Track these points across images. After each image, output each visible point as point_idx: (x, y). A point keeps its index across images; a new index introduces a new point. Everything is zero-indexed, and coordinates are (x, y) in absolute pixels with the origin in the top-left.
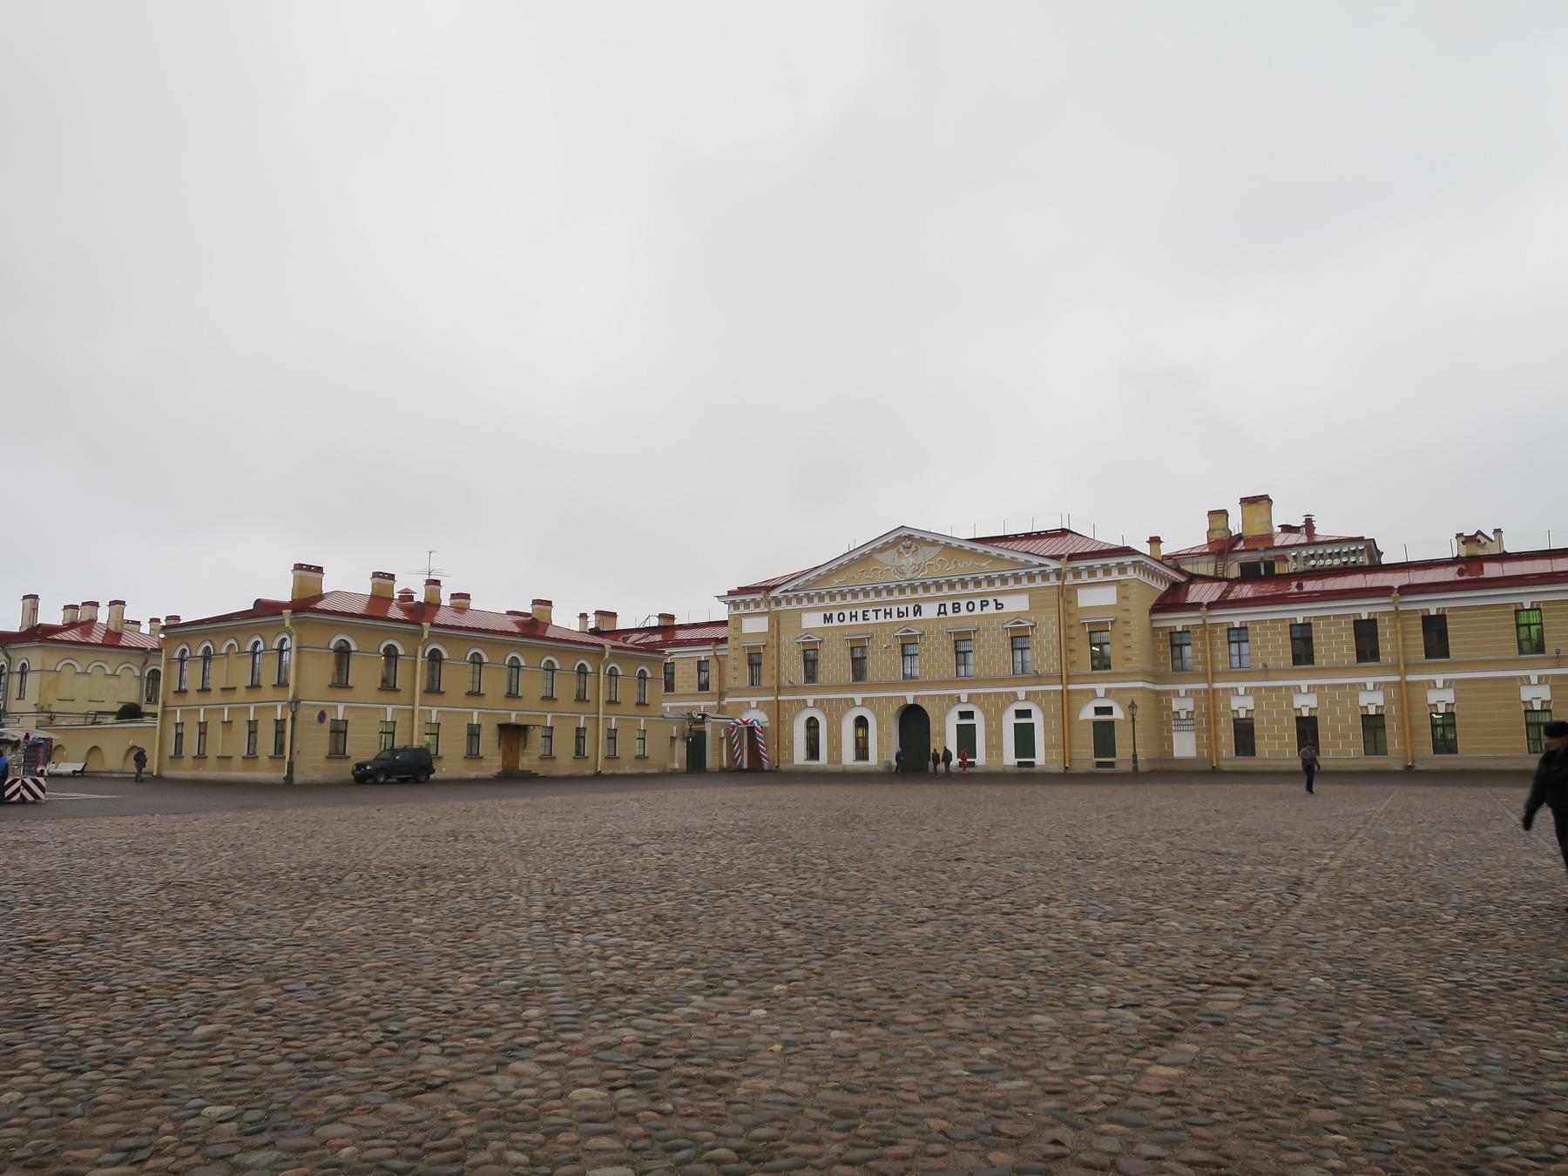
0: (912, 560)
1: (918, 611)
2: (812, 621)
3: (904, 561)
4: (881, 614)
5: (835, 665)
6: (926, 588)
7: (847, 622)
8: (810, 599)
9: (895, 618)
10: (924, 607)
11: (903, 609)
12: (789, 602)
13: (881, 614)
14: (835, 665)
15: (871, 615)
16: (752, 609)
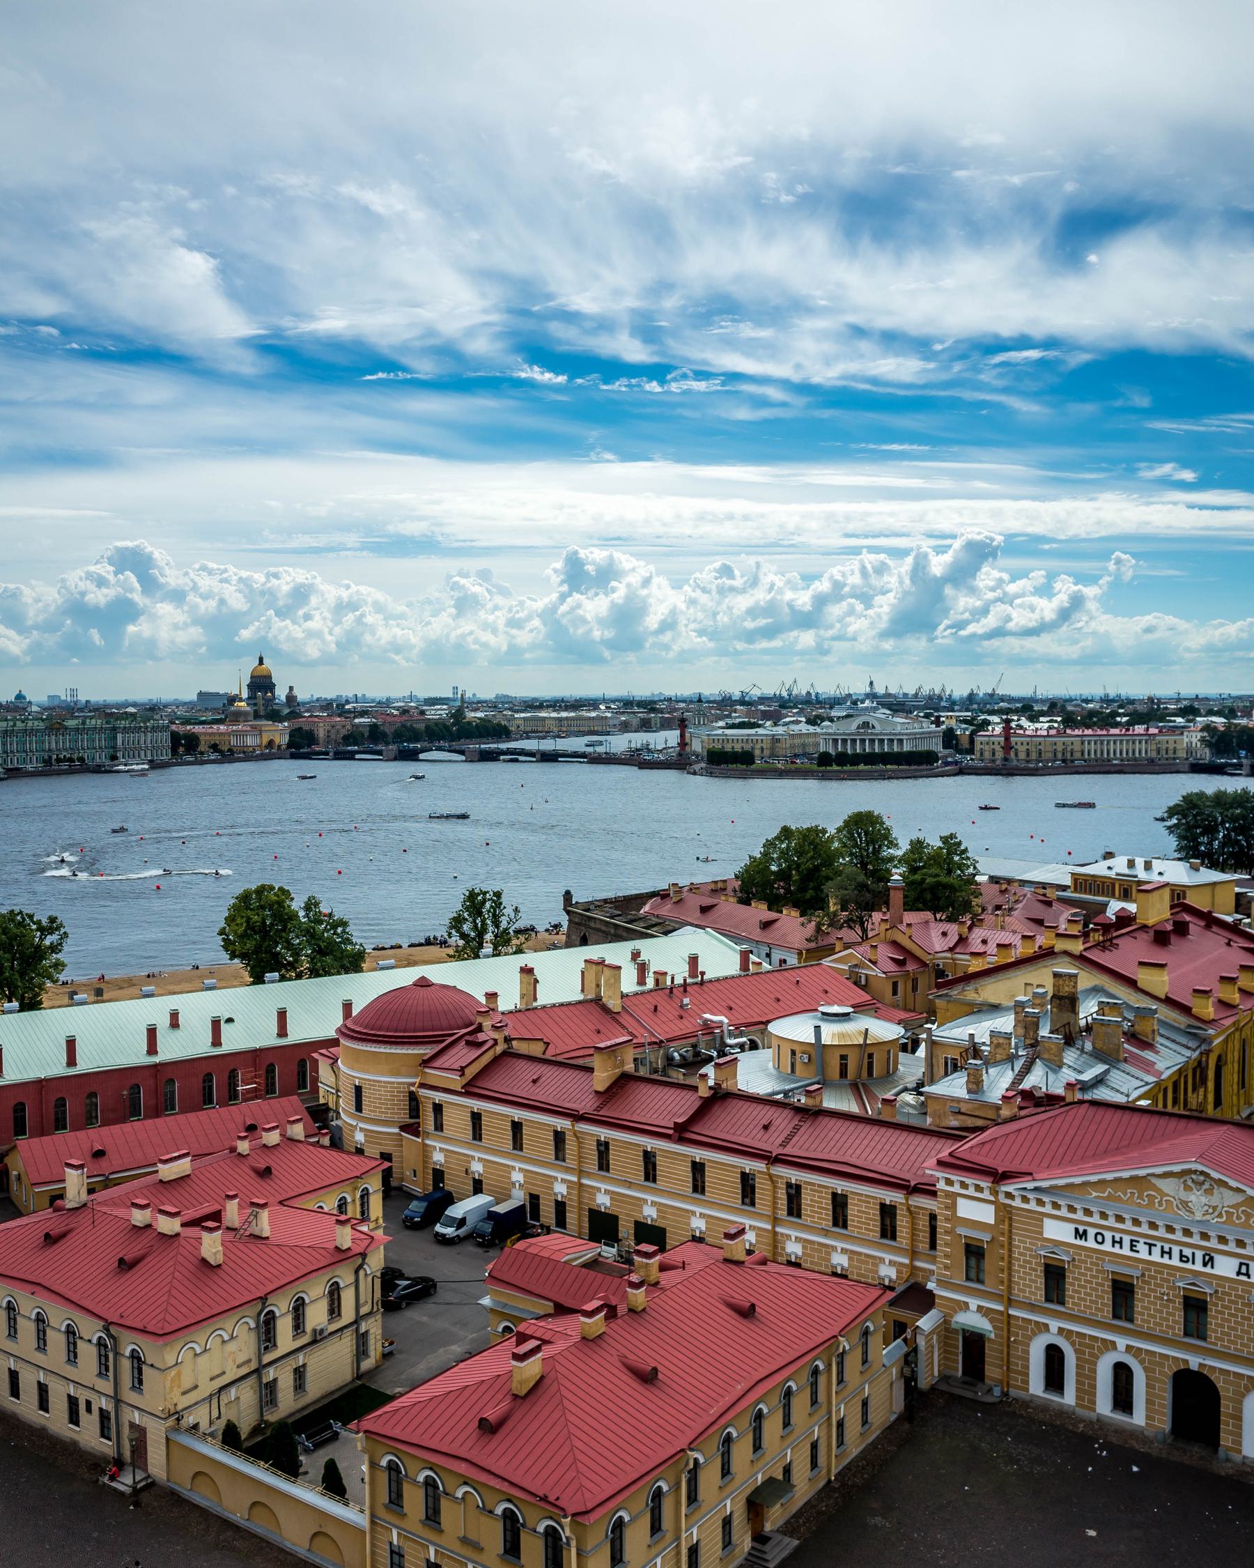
0: (1204, 1200)
1: (1209, 1261)
2: (1057, 1231)
3: (1193, 1198)
4: (1156, 1251)
5: (1088, 1291)
6: (1222, 1240)
7: (1107, 1247)
8: (1056, 1206)
9: (1175, 1262)
10: (1217, 1258)
11: (1188, 1252)
12: (1025, 1199)
13: (1156, 1251)
14: (1088, 1291)
15: (1142, 1247)
16: (971, 1191)
